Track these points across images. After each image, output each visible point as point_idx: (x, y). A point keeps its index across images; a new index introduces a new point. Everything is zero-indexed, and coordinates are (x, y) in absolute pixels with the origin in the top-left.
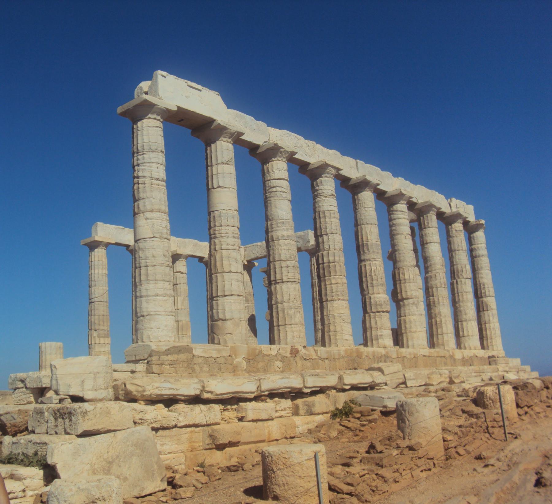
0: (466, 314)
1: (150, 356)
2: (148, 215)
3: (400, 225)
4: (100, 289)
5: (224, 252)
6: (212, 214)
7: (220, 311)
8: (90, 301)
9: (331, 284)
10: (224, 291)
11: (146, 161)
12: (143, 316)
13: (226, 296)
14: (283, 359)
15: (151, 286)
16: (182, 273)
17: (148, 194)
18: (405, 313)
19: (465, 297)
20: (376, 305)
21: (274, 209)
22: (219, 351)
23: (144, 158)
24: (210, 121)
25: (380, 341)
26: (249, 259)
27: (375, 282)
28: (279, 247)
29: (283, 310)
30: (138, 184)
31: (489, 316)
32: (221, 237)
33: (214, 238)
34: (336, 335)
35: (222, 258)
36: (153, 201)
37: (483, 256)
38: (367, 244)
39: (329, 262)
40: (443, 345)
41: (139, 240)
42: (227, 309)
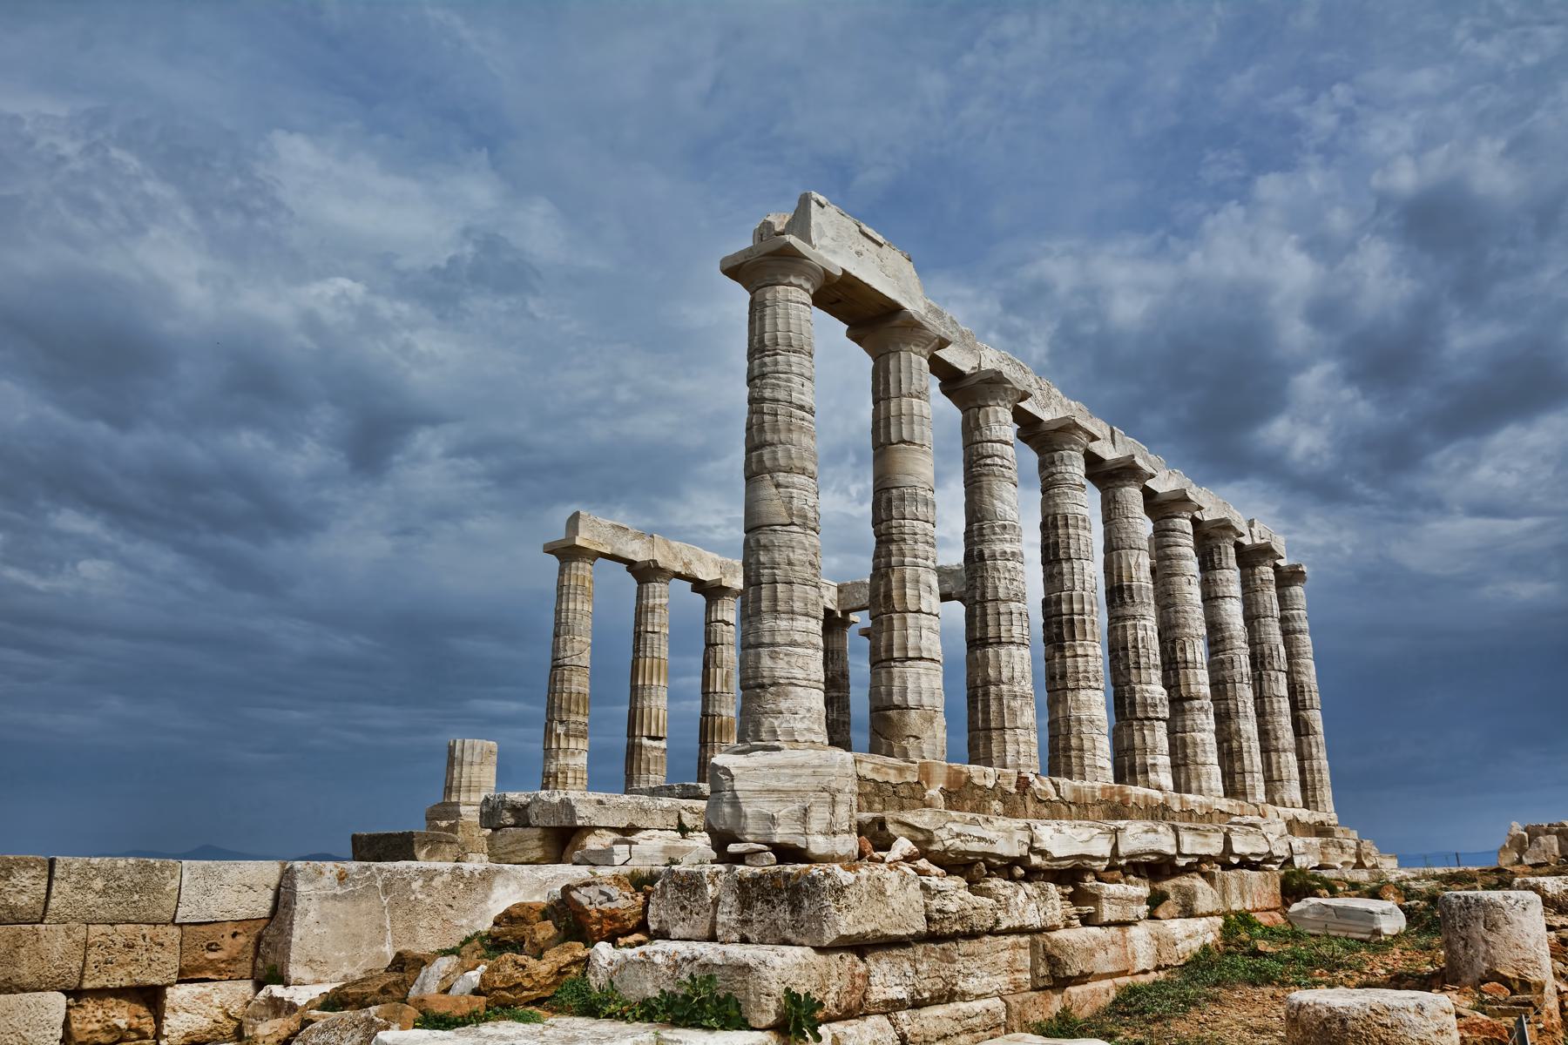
0: (1277, 738)
2: (782, 477)
3: (1180, 557)
5: (909, 572)
7: (895, 690)
9: (1076, 656)
10: (905, 649)
11: (780, 368)
14: (1005, 796)
15: (783, 624)
17: (783, 437)
18: (1184, 726)
19: (1276, 706)
20: (1145, 705)
21: (986, 498)
22: (900, 770)
23: (776, 363)
24: (894, 309)
25: (1151, 776)
27: (1143, 660)
29: (1000, 698)
31: (1310, 745)
34: (1082, 758)
35: (903, 581)
36: (793, 450)
37: (1301, 632)
38: (1130, 587)
40: (1244, 794)
41: (759, 527)
42: (910, 685)
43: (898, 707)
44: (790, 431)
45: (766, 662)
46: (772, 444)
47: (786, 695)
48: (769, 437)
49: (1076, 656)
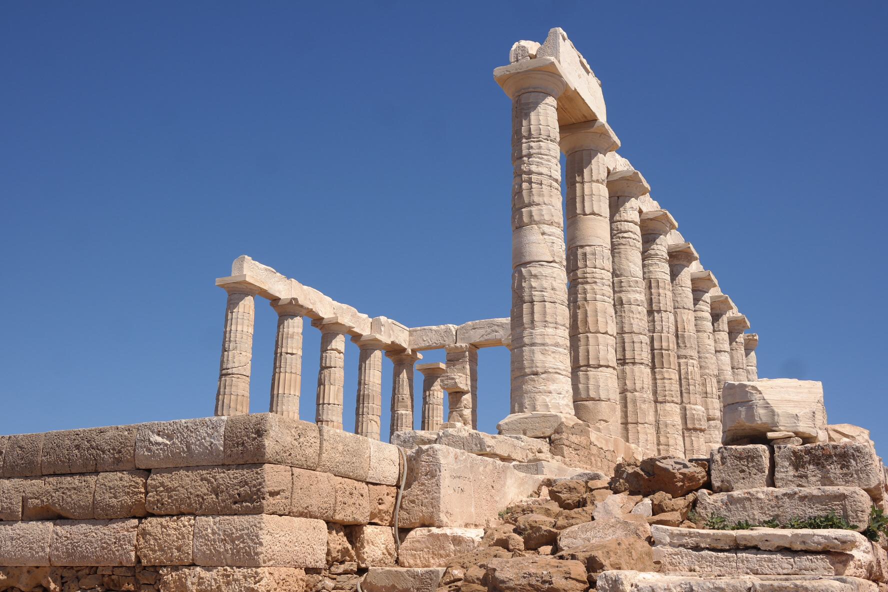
1: (558, 431)
2: (546, 228)
4: (241, 357)
5: (599, 304)
6: (580, 251)
7: (591, 387)
8: (224, 372)
9: (664, 379)
11: (543, 151)
12: (536, 374)
13: (601, 366)
15: (550, 331)
16: (340, 352)
17: (546, 200)
26: (416, 347)
28: (631, 315)
29: (634, 401)
32: (595, 282)
33: (582, 284)
39: (661, 349)
41: (530, 263)
43: (593, 399)
44: (551, 196)
45: (538, 357)
46: (538, 204)
47: (554, 381)
48: (536, 199)
49: (664, 379)
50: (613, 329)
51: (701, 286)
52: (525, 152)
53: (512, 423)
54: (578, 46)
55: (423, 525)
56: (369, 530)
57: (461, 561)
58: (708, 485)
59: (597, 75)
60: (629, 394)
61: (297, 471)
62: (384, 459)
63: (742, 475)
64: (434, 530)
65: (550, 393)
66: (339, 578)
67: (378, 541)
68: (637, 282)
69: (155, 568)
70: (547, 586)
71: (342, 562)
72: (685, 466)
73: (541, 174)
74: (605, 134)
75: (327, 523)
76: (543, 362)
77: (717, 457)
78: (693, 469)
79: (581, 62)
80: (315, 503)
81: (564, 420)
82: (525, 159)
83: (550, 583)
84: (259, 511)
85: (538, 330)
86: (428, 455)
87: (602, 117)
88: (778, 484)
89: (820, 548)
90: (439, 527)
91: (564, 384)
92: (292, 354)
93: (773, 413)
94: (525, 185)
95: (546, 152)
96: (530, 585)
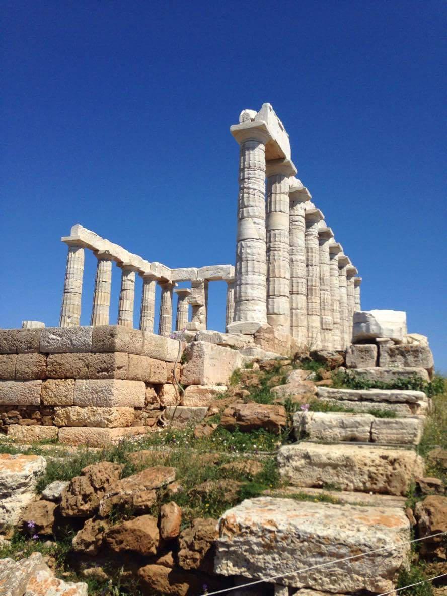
1: (258, 332)
4: (76, 282)
6: (272, 232)
7: (275, 307)
8: (66, 291)
11: (256, 176)
12: (248, 300)
13: (281, 296)
16: (132, 282)
17: (257, 204)
26: (174, 280)
28: (297, 268)
29: (297, 315)
30: (249, 194)
32: (280, 250)
33: (273, 250)
39: (312, 286)
41: (246, 239)
43: (276, 314)
45: (249, 291)
46: (252, 207)
48: (251, 203)
49: (312, 302)
50: (288, 276)
51: (334, 251)
52: (246, 176)
53: (234, 327)
54: (278, 114)
55: (194, 384)
56: (166, 387)
57: (217, 404)
58: (344, 365)
59: (287, 131)
60: (294, 311)
61: (131, 356)
62: (173, 349)
63: (362, 360)
64: (200, 386)
65: (255, 310)
66: (151, 412)
67: (170, 392)
68: (301, 250)
69: (52, 407)
70: (267, 419)
71: (152, 404)
72: (333, 355)
73: (254, 189)
74: (289, 166)
75: (146, 383)
76: (252, 294)
77: (350, 351)
78: (338, 357)
79: (279, 123)
80: (140, 373)
81: (262, 325)
82: (246, 180)
83: (269, 417)
84: (111, 377)
85: (250, 276)
86: (198, 347)
87: (288, 156)
88: (381, 365)
89: (405, 400)
90: (203, 385)
91: (262, 306)
92: (105, 282)
93: (380, 328)
94: (246, 195)
95: (258, 177)
96: (258, 418)
